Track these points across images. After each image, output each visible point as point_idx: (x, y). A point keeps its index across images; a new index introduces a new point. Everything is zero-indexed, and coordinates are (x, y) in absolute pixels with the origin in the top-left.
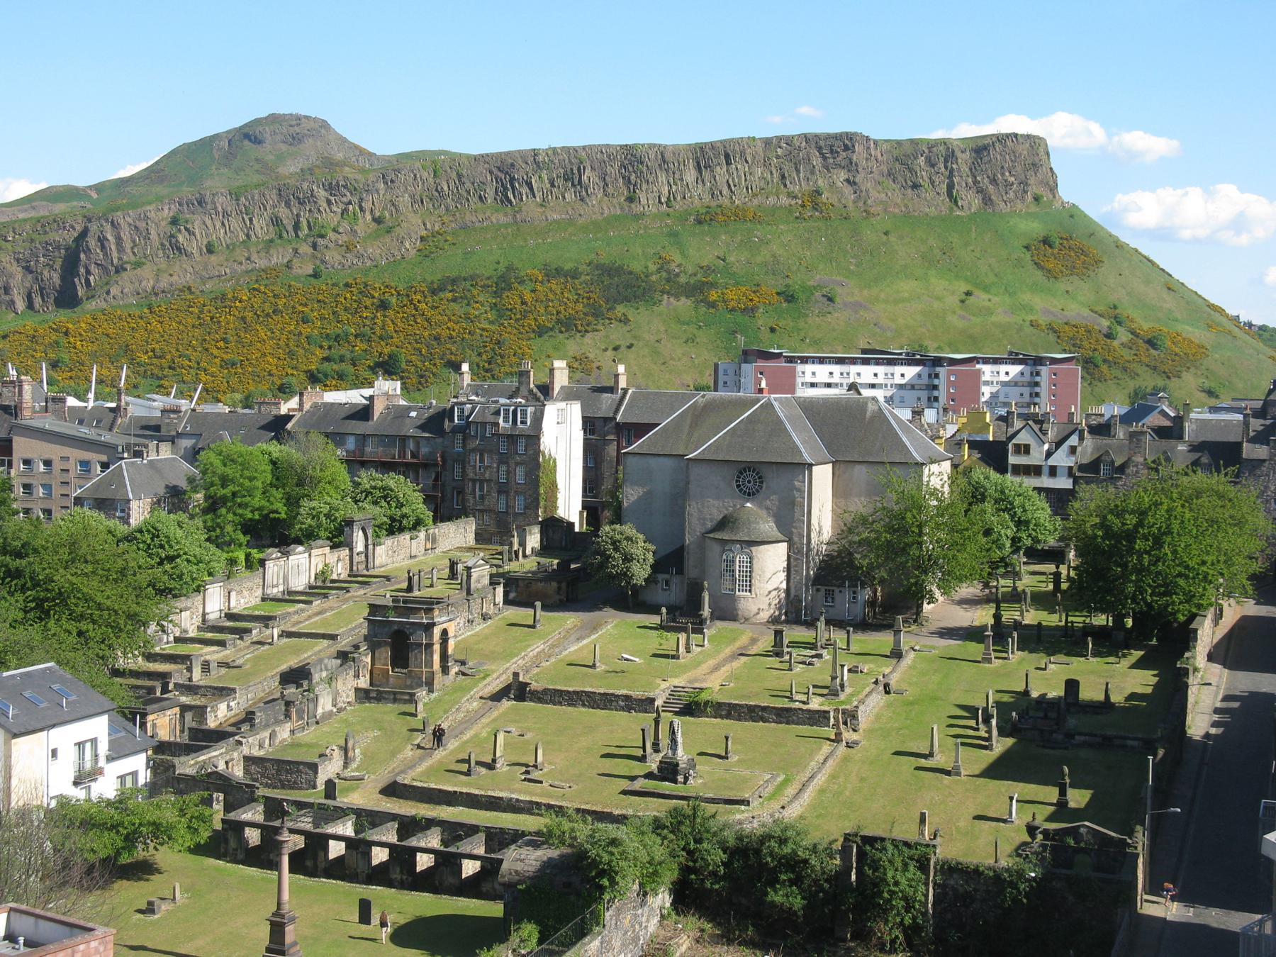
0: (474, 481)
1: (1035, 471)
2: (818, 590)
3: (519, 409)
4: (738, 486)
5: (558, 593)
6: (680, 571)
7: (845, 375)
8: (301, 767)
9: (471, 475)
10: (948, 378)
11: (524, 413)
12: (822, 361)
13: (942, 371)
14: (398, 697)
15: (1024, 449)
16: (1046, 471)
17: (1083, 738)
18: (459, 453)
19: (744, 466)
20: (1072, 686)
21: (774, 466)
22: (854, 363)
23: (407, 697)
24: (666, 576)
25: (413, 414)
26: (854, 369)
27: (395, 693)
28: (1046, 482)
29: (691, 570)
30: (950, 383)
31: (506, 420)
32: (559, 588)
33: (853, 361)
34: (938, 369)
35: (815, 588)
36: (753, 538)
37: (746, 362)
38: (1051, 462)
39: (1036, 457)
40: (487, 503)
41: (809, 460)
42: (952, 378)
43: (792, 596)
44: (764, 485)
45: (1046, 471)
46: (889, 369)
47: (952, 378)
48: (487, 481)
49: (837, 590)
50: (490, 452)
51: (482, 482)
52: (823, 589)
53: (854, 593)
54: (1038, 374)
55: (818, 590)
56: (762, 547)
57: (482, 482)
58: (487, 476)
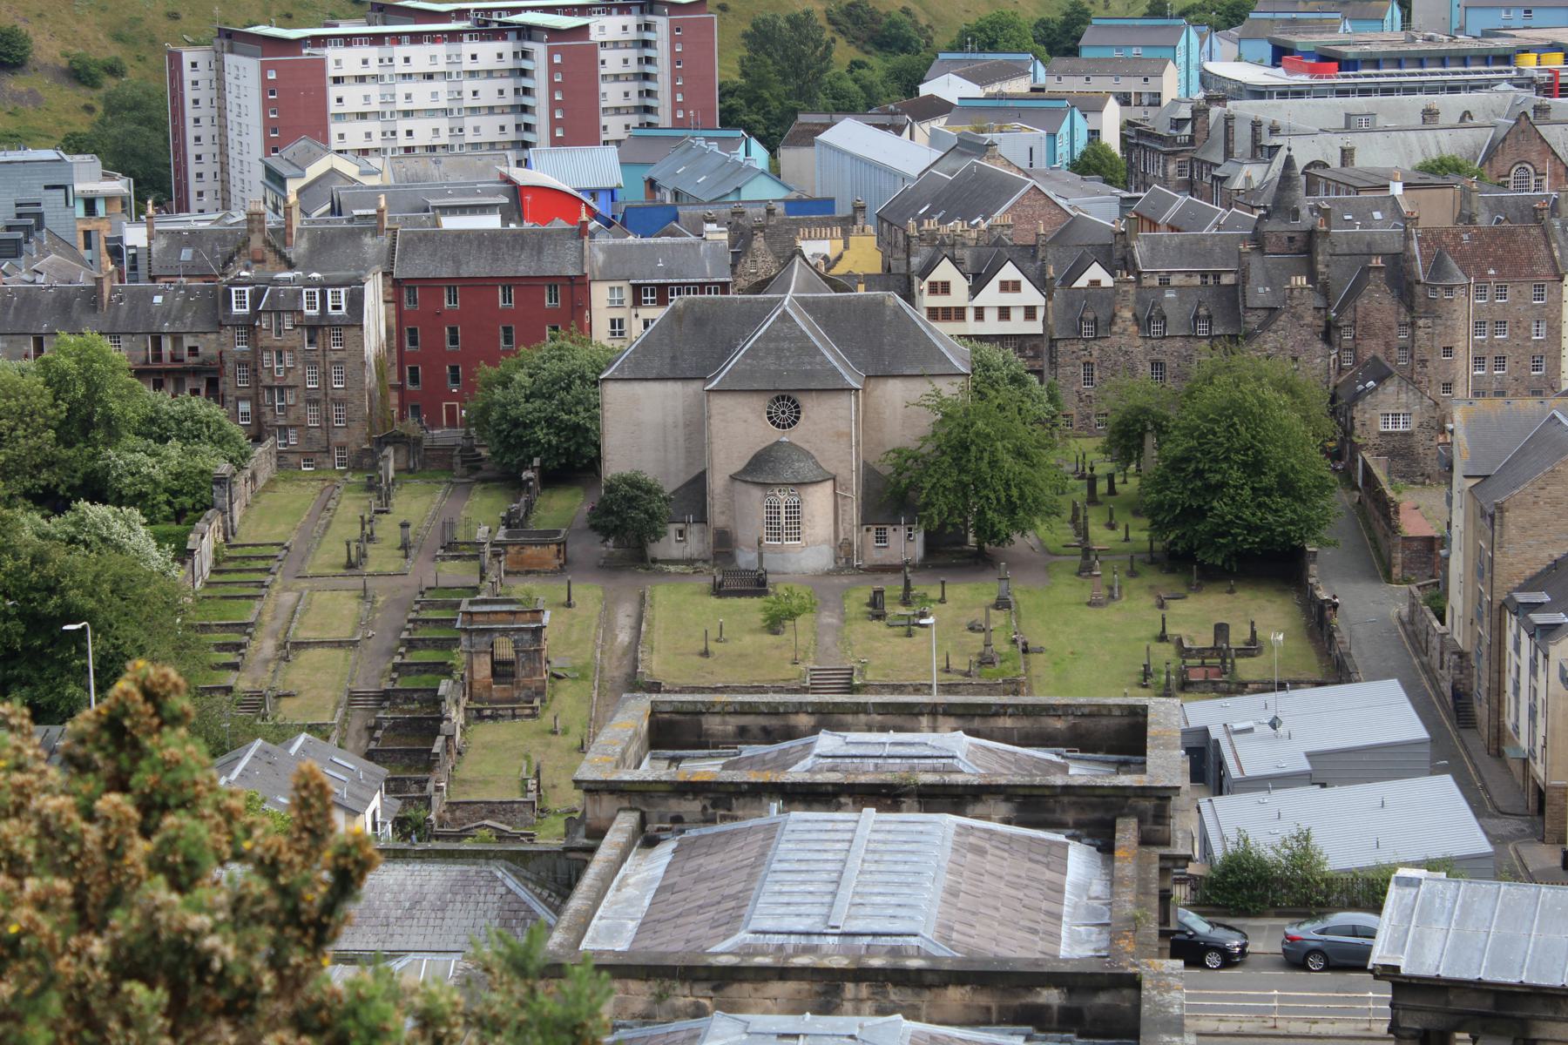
0: (270, 388)
1: (960, 313)
2: (868, 530)
3: (329, 291)
4: (770, 418)
5: (558, 558)
6: (702, 519)
7: (386, 61)
8: (516, 806)
9: (267, 381)
10: (550, 59)
11: (336, 296)
12: (348, 40)
13: (539, 49)
14: (518, 712)
15: (945, 288)
16: (970, 314)
17: (1256, 686)
18: (243, 353)
19: (776, 395)
20: (1221, 630)
21: (814, 394)
22: (399, 42)
23: (528, 711)
24: (681, 526)
25: (158, 299)
26: (400, 51)
27: (513, 709)
28: (971, 326)
29: (718, 516)
30: (553, 68)
31: (311, 305)
32: (559, 551)
33: (396, 38)
34: (528, 45)
35: (864, 528)
36: (800, 479)
37: (232, 51)
38: (980, 301)
39: (959, 295)
40: (292, 415)
41: (855, 385)
42: (557, 59)
43: (841, 537)
44: (803, 416)
45: (970, 314)
46: (453, 48)
47: (557, 59)
48: (290, 387)
49: (890, 529)
50: (291, 350)
51: (281, 389)
52: (873, 529)
53: (910, 529)
54: (648, 27)
55: (868, 530)
56: (811, 489)
57: (281, 389)
58: (289, 381)
